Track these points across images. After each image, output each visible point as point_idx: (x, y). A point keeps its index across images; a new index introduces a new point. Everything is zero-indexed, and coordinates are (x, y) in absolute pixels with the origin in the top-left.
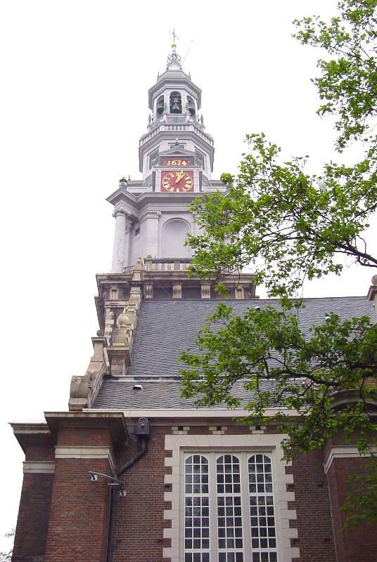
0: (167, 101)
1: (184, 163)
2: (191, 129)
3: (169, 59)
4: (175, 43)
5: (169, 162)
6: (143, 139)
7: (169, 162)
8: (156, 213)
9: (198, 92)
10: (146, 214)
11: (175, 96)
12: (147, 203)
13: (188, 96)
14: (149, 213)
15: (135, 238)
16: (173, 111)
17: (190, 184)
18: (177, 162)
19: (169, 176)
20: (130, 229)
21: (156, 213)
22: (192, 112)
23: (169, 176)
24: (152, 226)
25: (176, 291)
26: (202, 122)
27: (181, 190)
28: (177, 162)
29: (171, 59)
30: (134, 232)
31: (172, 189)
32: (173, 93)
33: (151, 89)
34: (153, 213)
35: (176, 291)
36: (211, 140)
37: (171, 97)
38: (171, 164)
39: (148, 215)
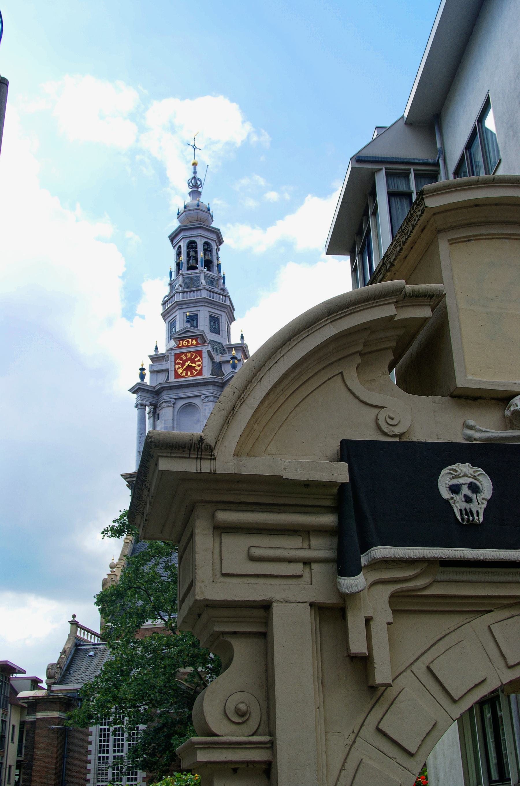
1: (194, 342)
2: (204, 294)
5: (181, 342)
6: (164, 304)
7: (181, 342)
9: (217, 233)
12: (164, 390)
14: (165, 402)
16: (189, 269)
17: (199, 366)
18: (188, 342)
19: (181, 359)
23: (181, 359)
27: (192, 373)
28: (188, 342)
29: (191, 184)
31: (184, 374)
34: (168, 402)
37: (188, 247)
38: (182, 343)
39: (164, 404)
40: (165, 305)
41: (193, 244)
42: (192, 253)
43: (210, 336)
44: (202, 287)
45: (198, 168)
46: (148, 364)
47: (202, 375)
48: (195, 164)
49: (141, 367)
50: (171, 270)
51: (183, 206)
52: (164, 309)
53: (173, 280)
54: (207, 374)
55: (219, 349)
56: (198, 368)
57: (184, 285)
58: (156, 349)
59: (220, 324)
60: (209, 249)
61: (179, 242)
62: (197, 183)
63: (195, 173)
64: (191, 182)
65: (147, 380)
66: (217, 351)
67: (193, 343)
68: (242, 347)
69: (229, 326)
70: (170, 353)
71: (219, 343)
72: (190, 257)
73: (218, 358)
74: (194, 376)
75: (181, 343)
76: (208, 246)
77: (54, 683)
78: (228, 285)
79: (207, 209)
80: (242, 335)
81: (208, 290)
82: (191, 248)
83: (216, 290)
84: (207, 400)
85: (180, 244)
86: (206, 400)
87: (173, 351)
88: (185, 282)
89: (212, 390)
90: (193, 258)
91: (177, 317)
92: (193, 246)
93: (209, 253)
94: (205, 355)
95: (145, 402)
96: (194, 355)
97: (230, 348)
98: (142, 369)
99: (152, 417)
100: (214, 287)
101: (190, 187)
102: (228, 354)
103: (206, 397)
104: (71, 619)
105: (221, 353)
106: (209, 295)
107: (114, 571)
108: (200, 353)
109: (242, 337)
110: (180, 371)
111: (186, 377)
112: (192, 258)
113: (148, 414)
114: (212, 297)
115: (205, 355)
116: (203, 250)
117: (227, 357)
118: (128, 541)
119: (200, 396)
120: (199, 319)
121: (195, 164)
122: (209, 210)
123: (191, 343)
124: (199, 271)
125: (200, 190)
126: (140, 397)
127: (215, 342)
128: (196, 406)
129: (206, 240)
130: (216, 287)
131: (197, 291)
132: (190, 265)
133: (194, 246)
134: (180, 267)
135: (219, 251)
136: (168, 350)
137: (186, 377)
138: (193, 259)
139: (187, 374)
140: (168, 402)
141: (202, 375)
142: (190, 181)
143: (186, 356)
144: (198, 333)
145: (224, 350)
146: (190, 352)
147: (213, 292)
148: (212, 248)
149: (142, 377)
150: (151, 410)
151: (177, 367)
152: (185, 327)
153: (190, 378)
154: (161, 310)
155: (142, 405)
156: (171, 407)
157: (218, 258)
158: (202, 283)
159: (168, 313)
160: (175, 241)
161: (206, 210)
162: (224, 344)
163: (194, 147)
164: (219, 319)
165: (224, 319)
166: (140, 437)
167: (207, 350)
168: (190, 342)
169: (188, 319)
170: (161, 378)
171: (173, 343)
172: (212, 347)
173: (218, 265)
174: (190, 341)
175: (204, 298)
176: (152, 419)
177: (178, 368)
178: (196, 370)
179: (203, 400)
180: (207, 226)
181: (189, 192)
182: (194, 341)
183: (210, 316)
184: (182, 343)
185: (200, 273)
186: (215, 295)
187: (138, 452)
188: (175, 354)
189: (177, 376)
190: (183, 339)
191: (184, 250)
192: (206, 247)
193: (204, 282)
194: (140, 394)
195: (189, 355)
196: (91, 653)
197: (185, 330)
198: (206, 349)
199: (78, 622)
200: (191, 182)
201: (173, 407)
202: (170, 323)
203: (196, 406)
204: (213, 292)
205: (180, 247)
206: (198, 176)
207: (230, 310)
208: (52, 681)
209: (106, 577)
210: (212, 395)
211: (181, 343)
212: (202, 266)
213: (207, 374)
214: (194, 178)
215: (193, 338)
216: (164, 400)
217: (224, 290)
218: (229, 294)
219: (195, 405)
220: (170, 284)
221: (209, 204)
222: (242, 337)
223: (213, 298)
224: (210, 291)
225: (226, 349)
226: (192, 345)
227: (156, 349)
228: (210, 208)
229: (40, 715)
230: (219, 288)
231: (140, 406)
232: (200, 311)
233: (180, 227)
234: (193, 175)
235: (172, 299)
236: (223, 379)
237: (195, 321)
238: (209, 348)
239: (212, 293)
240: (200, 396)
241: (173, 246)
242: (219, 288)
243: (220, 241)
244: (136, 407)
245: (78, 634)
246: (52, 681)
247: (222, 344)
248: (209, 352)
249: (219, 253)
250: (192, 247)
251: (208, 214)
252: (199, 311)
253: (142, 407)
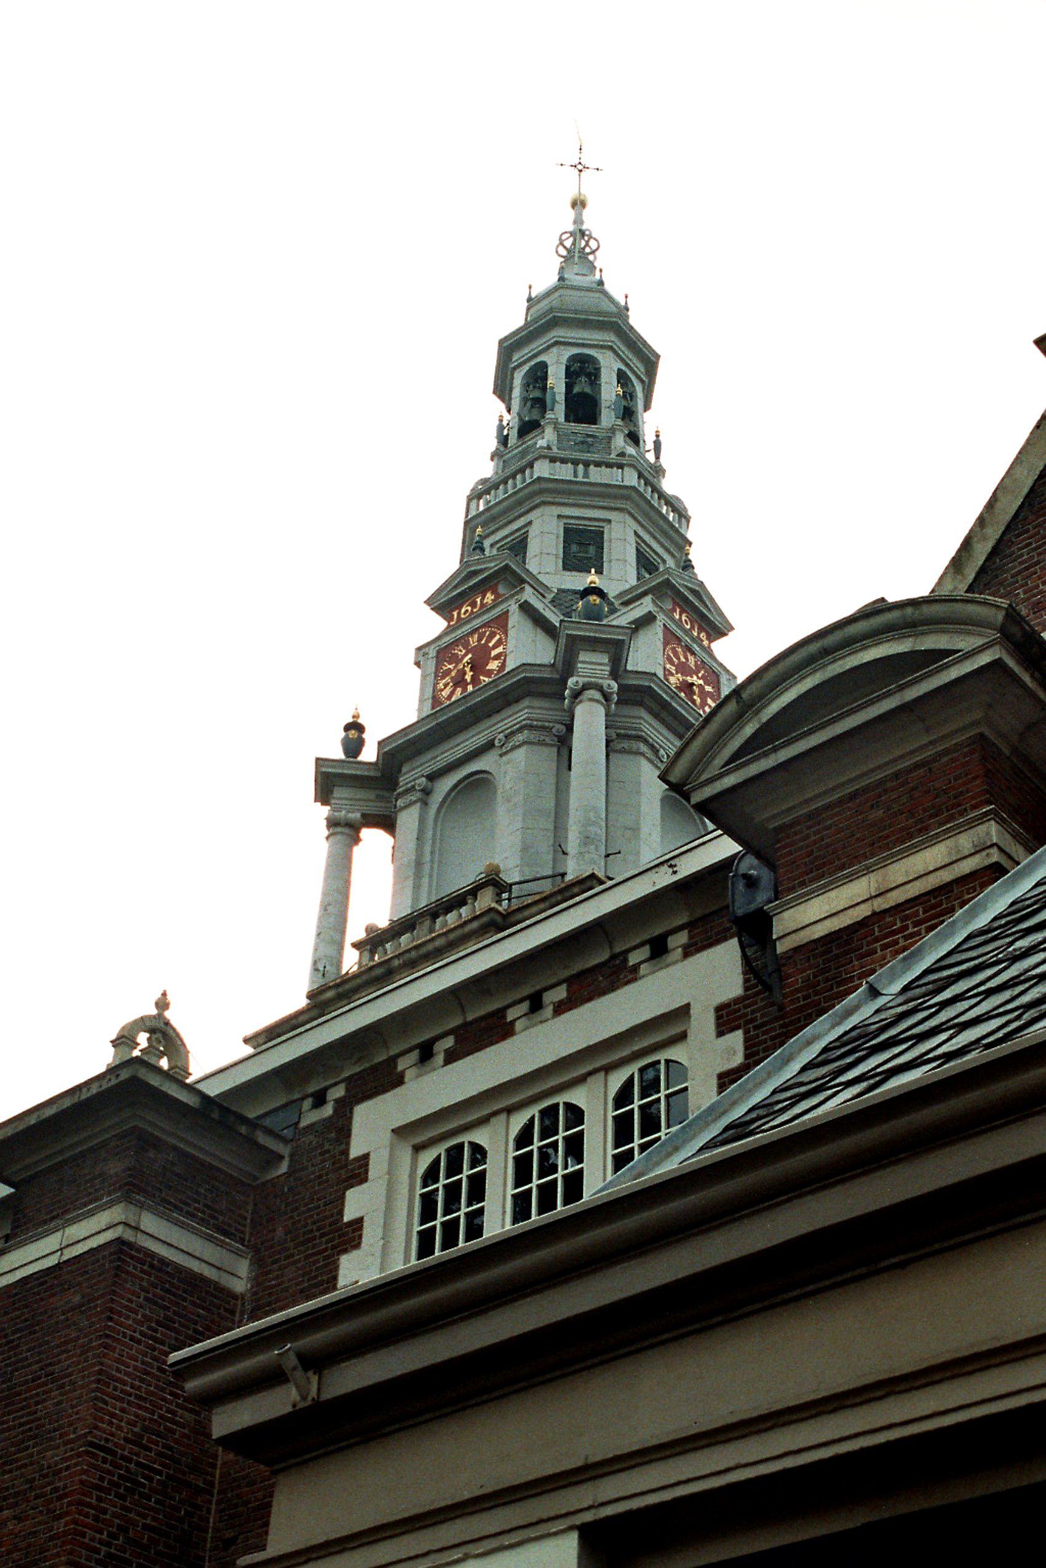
0: (556, 380)
2: (630, 478)
3: (561, 243)
6: (476, 496)
9: (649, 361)
13: (619, 370)
22: (628, 414)
26: (657, 457)
29: (568, 243)
32: (574, 359)
33: (506, 339)
36: (683, 515)
45: (586, 213)
48: (579, 204)
61: (535, 356)
63: (578, 221)
101: (564, 252)
121: (579, 204)
129: (624, 368)
221: (626, 297)
228: (630, 306)
234: (571, 228)
252: (609, 521)
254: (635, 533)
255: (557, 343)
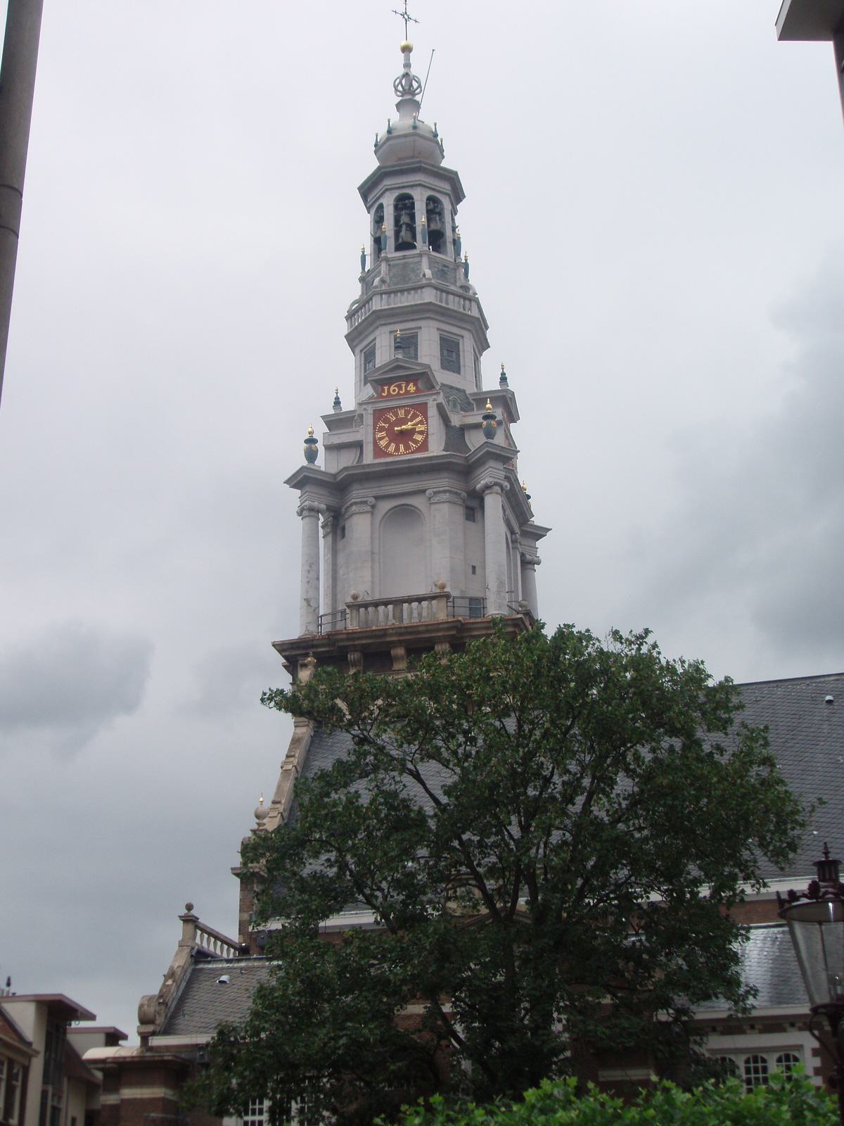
1: (412, 388)
2: (429, 296)
4: (410, 42)
5: (386, 388)
6: (351, 316)
7: (386, 388)
8: (365, 502)
9: (452, 179)
10: (352, 505)
11: (404, 204)
14: (356, 503)
15: (340, 544)
16: (401, 246)
17: (421, 433)
18: (400, 387)
19: (386, 420)
20: (333, 525)
21: (365, 502)
23: (386, 420)
24: (360, 526)
25: (398, 658)
27: (407, 447)
28: (400, 388)
29: (400, 88)
30: (339, 532)
31: (392, 448)
34: (362, 503)
35: (398, 658)
37: (396, 208)
38: (389, 389)
39: (354, 508)
40: (353, 318)
41: (407, 201)
42: (405, 219)
43: (443, 377)
44: (424, 281)
46: (320, 430)
47: (427, 450)
48: (407, 50)
49: (307, 436)
50: (363, 252)
51: (386, 129)
52: (352, 326)
53: (369, 270)
54: (436, 448)
55: (459, 401)
56: (419, 438)
57: (390, 280)
58: (337, 402)
59: (461, 353)
60: (437, 210)
62: (411, 85)
63: (407, 65)
64: (400, 82)
65: (321, 462)
66: (455, 406)
67: (408, 389)
68: (504, 398)
69: (477, 358)
70: (365, 409)
71: (458, 389)
72: (401, 226)
73: (456, 420)
74: (412, 453)
75: (386, 390)
76: (436, 205)
77: (154, 1034)
78: (473, 280)
79: (432, 134)
80: (503, 374)
81: (436, 288)
82: (402, 209)
83: (452, 288)
84: (438, 498)
85: (381, 201)
86: (436, 499)
87: (370, 406)
88: (391, 274)
89: (447, 480)
90: (407, 227)
91: (378, 342)
92: (406, 204)
93: (438, 218)
94: (432, 412)
95: (316, 503)
96: (412, 412)
97: (480, 399)
98: (311, 441)
99: (331, 535)
100: (447, 282)
102: (477, 410)
103: (435, 493)
104: (184, 912)
105: (462, 409)
106: (438, 296)
107: (264, 824)
108: (423, 408)
109: (503, 379)
110: (383, 443)
111: (396, 455)
112: (404, 228)
113: (323, 527)
114: (444, 302)
115: (432, 412)
116: (425, 212)
117: (476, 417)
118: (290, 767)
119: (424, 491)
120: (419, 343)
121: (407, 50)
122: (436, 135)
123: (406, 389)
124: (418, 252)
125: (418, 98)
126: (307, 494)
127: (451, 387)
128: (417, 510)
130: (453, 284)
131: (415, 289)
132: (400, 240)
133: (409, 204)
134: (383, 246)
135: (456, 214)
136: (360, 404)
137: (396, 455)
138: (406, 230)
139: (397, 449)
140: (362, 503)
141: (427, 450)
142: (398, 81)
143: (396, 414)
144: (419, 370)
145: (469, 403)
146: (404, 406)
147: (448, 293)
148: (442, 209)
149: (311, 455)
150: (329, 520)
151: (379, 435)
152: (393, 358)
153: (401, 454)
154: (344, 328)
155: (311, 509)
156: (367, 512)
157: (454, 228)
158: (424, 275)
159: (360, 334)
160: (371, 198)
161: (431, 136)
162: (467, 392)
163: (405, 16)
164: (458, 344)
165: (467, 345)
166: (309, 572)
167: (436, 402)
168: (404, 388)
169: (398, 342)
170: (347, 460)
171: (369, 391)
172: (446, 398)
173: (454, 240)
174: (403, 385)
175: (430, 303)
176: (330, 538)
177: (381, 439)
178: (416, 442)
179: (430, 499)
180: (433, 166)
181: (396, 103)
182: (411, 385)
183: (442, 339)
184: (389, 389)
185: (420, 255)
186: (451, 297)
187: (305, 599)
188: (374, 411)
189: (379, 452)
190: (389, 382)
191: (389, 213)
192: (431, 206)
193: (428, 273)
194: (308, 488)
195: (401, 413)
196: (224, 978)
197: (393, 366)
198: (435, 400)
199: (198, 919)
200: (400, 82)
201: (372, 513)
202: (363, 354)
203: (417, 510)
204: (448, 293)
205: (381, 207)
206: (414, 71)
207: (478, 327)
208: (150, 1028)
209: (250, 834)
210: (447, 488)
211: (386, 390)
212: (424, 242)
213: (436, 448)
214: (406, 75)
215: (409, 379)
216: (353, 500)
217: (466, 288)
218: (476, 296)
219: (413, 508)
220: (362, 280)
221: (435, 125)
222: (503, 379)
223: (447, 303)
224: (442, 291)
225: (472, 402)
226: (407, 392)
227: (337, 402)
229: (128, 1093)
230: (458, 284)
231: (307, 511)
232: (423, 329)
233: (379, 168)
234: (402, 71)
235: (367, 306)
236: (469, 458)
237: (412, 351)
238: (441, 399)
239: (444, 295)
240: (424, 491)
241: (368, 206)
242: (458, 284)
243: (457, 195)
244: (300, 513)
245: (198, 940)
246: (150, 1028)
247: (464, 391)
248: (440, 407)
249: (456, 218)
250: (405, 207)
251: (433, 144)
252: (421, 328)
253: (313, 513)
254: (438, 329)
255: (387, 190)
